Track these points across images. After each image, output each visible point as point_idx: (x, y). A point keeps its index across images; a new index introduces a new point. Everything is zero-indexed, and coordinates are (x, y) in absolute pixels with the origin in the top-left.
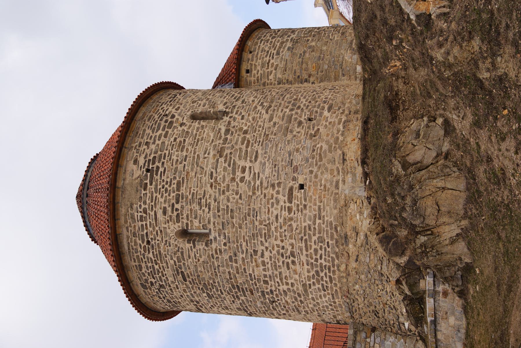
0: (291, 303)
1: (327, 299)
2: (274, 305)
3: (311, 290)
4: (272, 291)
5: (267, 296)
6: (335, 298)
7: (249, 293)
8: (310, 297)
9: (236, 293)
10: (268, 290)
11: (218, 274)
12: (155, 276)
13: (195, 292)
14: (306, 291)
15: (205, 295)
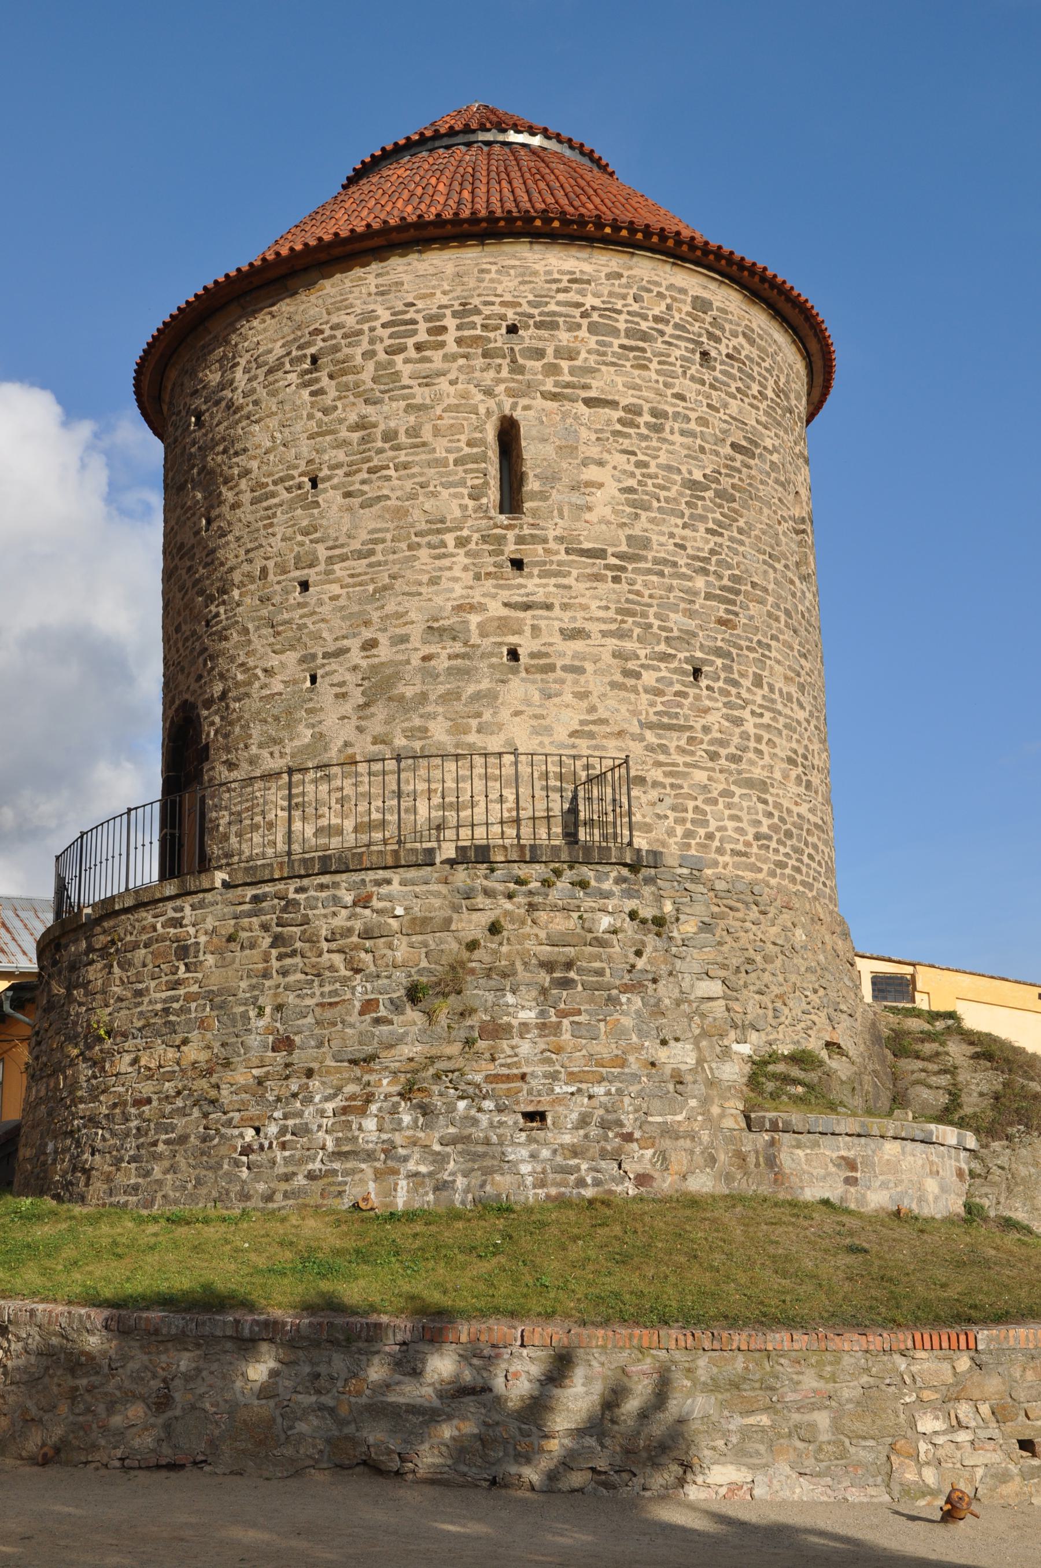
0: (702, 722)
1: (730, 833)
2: (685, 666)
3: (755, 799)
4: (735, 683)
5: (719, 662)
6: (736, 859)
7: (721, 614)
8: (733, 788)
9: (720, 577)
10: (736, 676)
11: (761, 557)
12: (736, 364)
13: (702, 450)
14: (749, 783)
15: (698, 475)
